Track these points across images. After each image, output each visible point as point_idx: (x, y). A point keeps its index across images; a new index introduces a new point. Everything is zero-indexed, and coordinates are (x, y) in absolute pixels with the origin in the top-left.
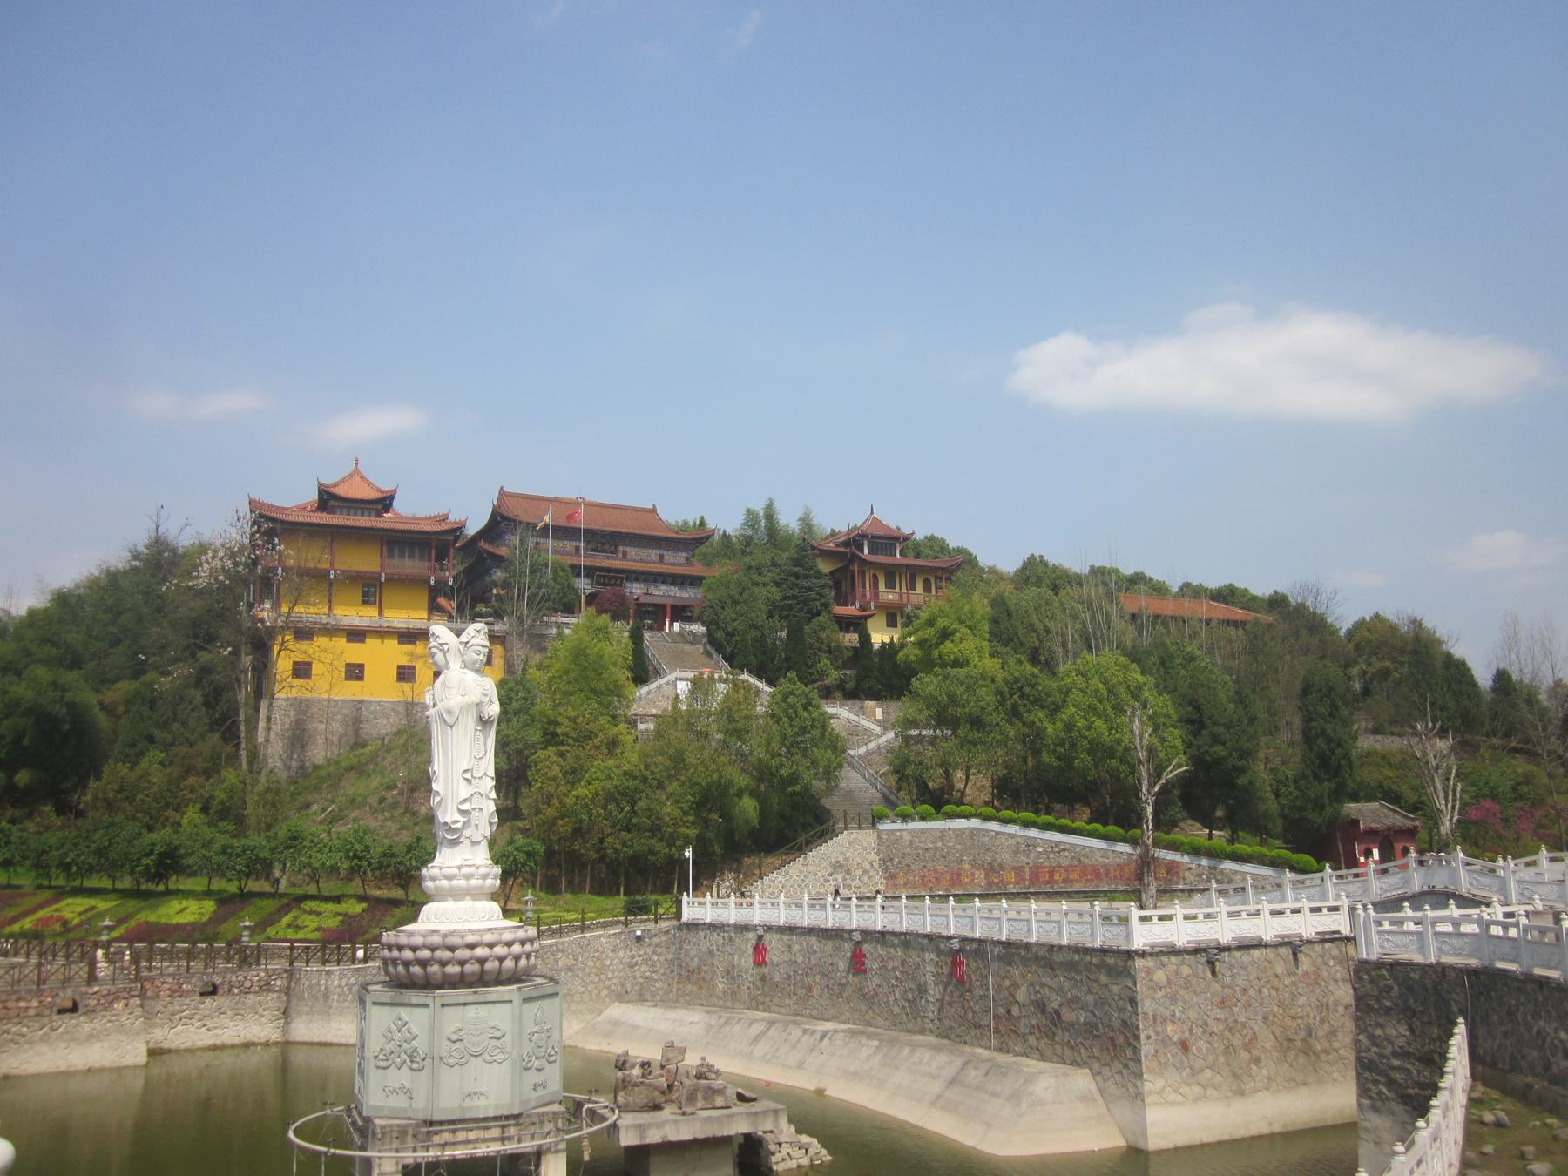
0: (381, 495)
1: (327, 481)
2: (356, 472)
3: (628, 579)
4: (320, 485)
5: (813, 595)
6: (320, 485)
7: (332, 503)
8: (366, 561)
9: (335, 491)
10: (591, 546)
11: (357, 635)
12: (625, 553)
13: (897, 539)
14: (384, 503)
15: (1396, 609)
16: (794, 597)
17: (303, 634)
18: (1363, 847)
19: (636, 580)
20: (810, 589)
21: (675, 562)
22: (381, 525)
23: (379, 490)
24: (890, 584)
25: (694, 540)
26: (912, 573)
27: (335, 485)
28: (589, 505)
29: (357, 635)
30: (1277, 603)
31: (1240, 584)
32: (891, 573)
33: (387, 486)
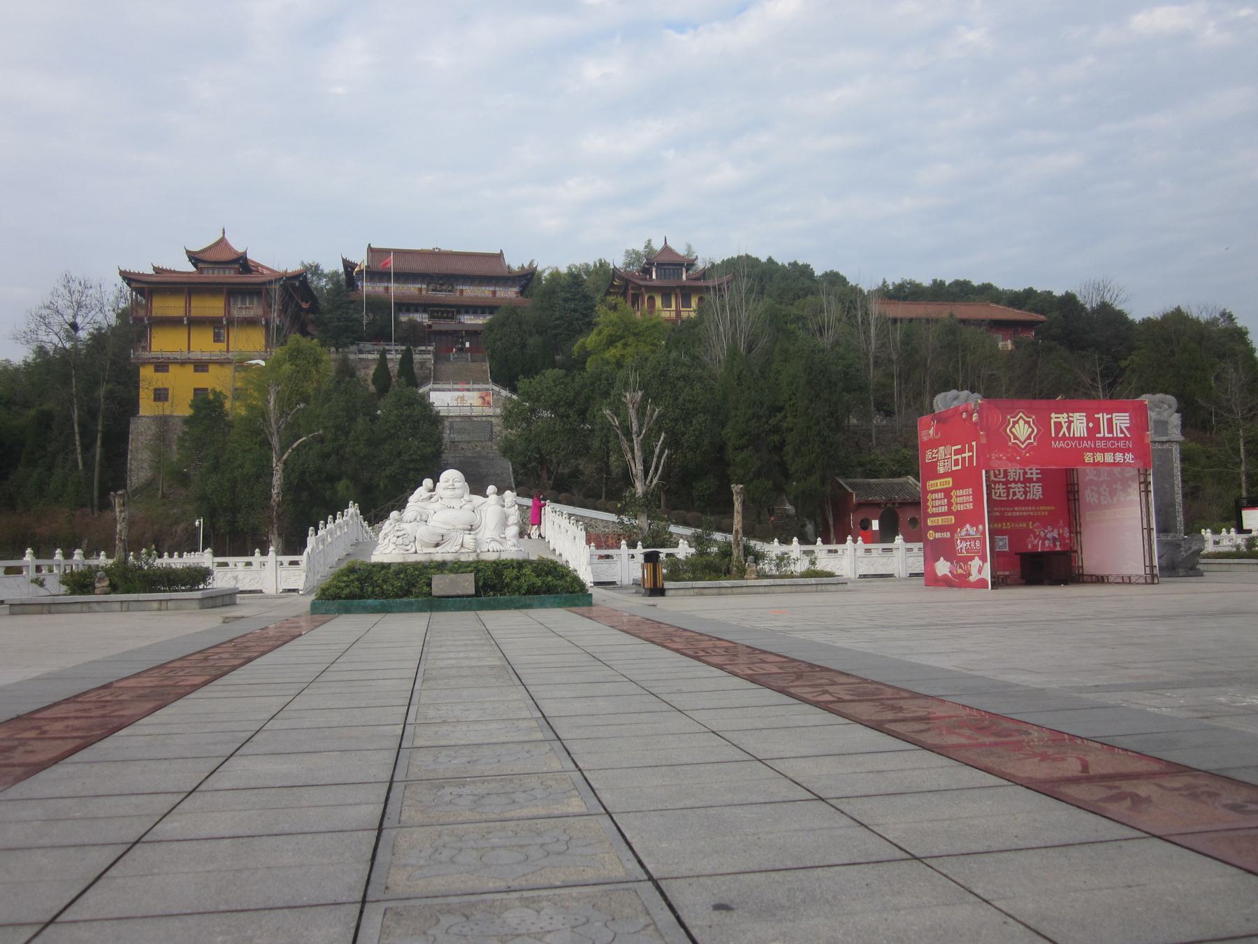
0: (235, 257)
1: (196, 248)
2: (222, 242)
3: (459, 312)
4: (188, 252)
5: (577, 315)
6: (188, 252)
7: (200, 265)
8: (213, 307)
9: (200, 256)
10: (431, 287)
11: (201, 366)
12: (462, 291)
13: (682, 265)
14: (242, 263)
15: (1201, 304)
16: (561, 318)
17: (162, 366)
18: (860, 518)
19: (467, 312)
20: (575, 311)
21: (509, 293)
22: (254, 280)
23: (236, 252)
24: (667, 303)
25: (527, 279)
26: (685, 293)
27: (203, 251)
28: (398, 252)
29: (201, 366)
30: (1069, 300)
31: (1039, 288)
32: (666, 293)
33: (240, 249)
